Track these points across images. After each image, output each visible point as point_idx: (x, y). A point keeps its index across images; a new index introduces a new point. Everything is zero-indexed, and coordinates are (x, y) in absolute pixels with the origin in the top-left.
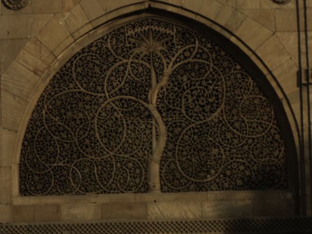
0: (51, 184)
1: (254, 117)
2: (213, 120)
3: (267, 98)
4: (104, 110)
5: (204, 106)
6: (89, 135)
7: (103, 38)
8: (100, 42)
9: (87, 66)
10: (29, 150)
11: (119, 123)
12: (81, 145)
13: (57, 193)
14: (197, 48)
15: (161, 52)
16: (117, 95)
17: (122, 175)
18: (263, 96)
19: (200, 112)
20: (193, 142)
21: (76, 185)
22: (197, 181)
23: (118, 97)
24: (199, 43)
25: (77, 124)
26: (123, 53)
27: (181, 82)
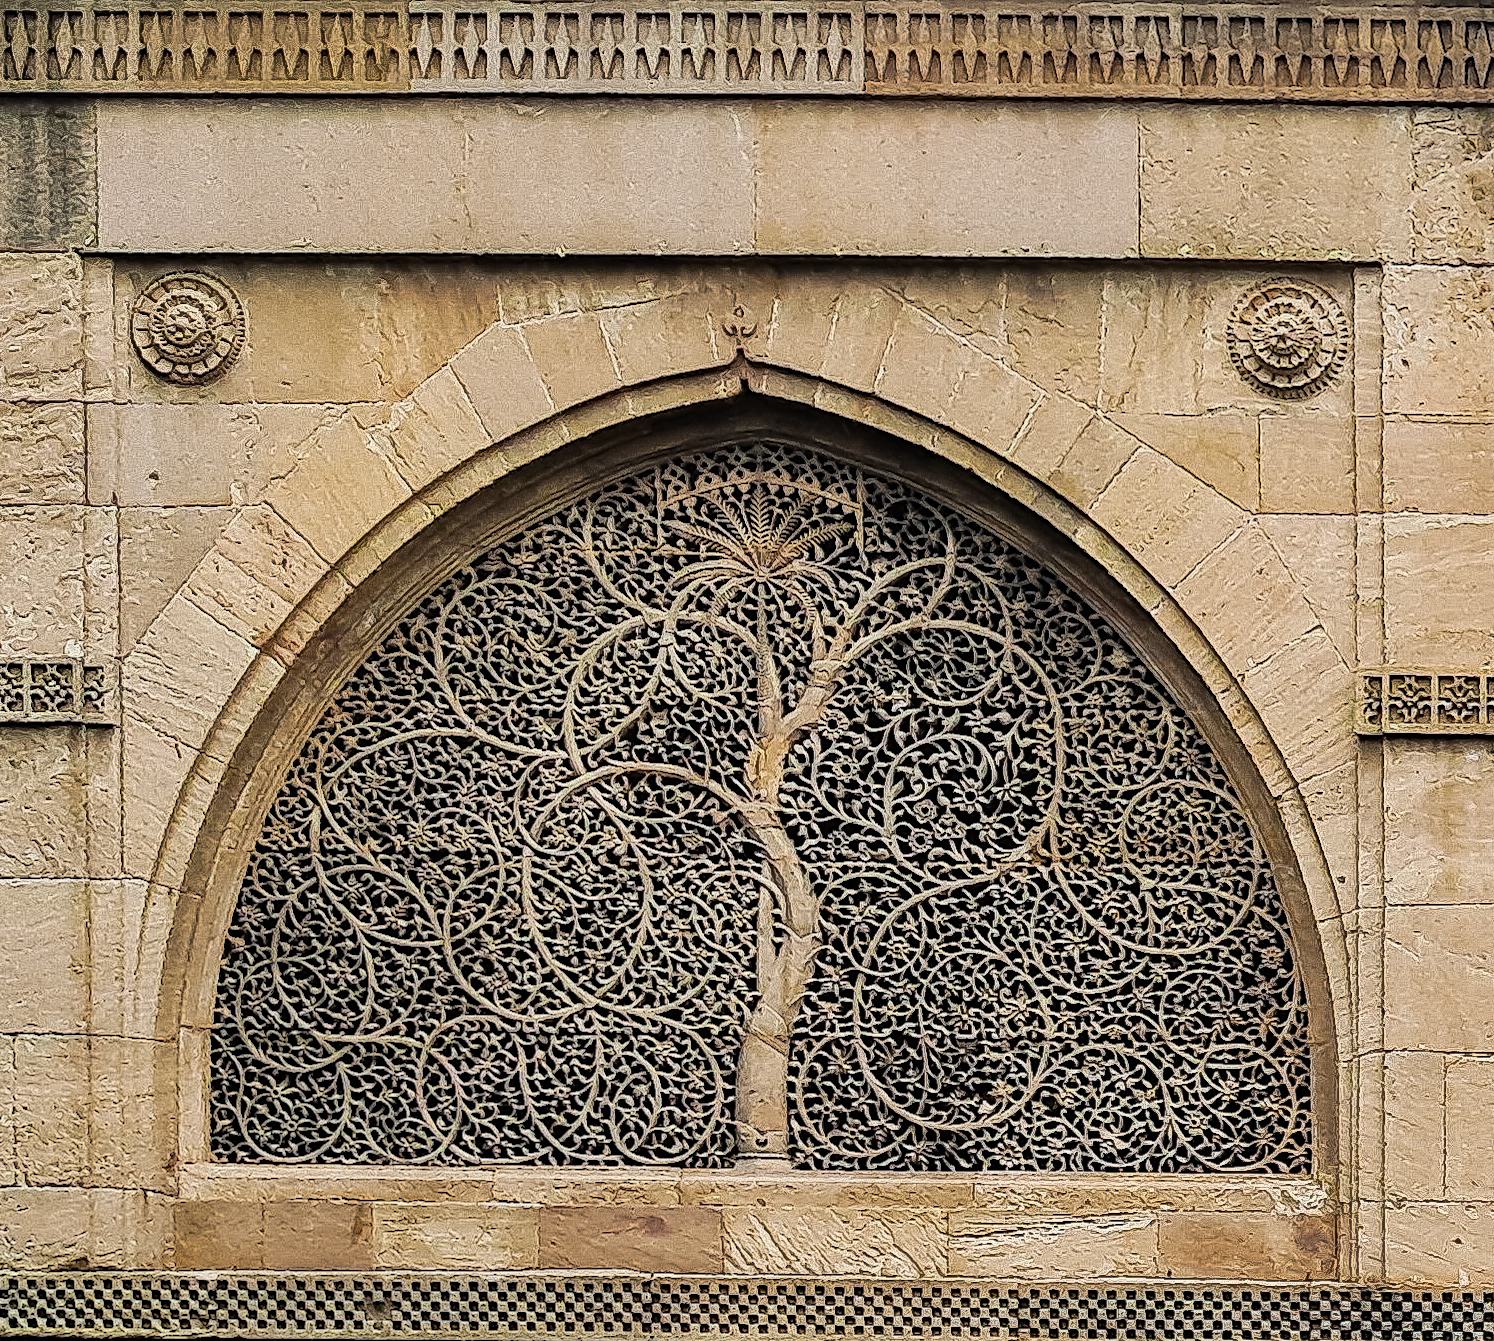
0: (338, 1116)
1: (1177, 871)
2: (1008, 878)
3: (1231, 791)
4: (562, 816)
5: (975, 817)
8: (550, 533)
9: (498, 630)
13: (364, 1157)
14: (949, 571)
15: (804, 585)
16: (618, 757)
17: (628, 1091)
18: (1219, 784)
19: (958, 842)
20: (924, 963)
21: (441, 1122)
22: (934, 1125)
23: (618, 767)
24: (960, 553)
25: (448, 874)
26: (646, 584)
27: (882, 712)
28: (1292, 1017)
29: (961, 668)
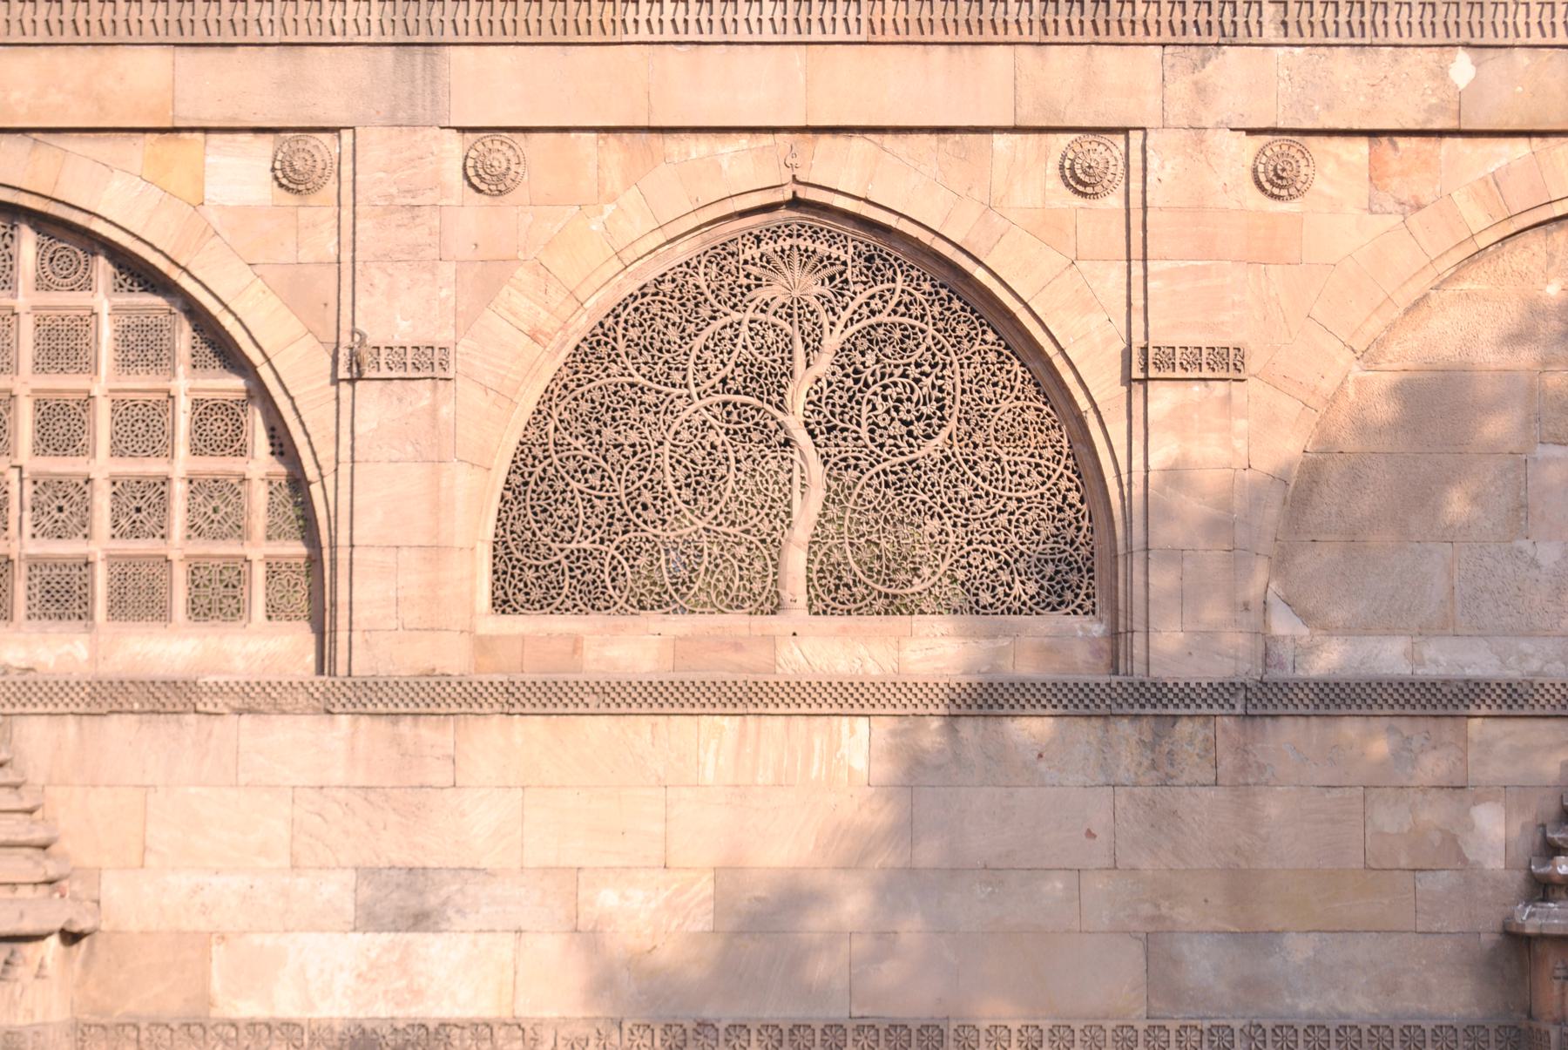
0: (561, 588)
3: (1052, 408)
4: (686, 425)
5: (911, 423)
6: (651, 480)
7: (688, 264)
10: (515, 513)
11: (719, 455)
12: (633, 503)
13: (576, 610)
14: (898, 292)
16: (717, 392)
18: (1045, 404)
19: (902, 436)
20: (883, 504)
22: (890, 591)
25: (624, 456)
27: (861, 367)
28: (1084, 530)
29: (903, 342)
